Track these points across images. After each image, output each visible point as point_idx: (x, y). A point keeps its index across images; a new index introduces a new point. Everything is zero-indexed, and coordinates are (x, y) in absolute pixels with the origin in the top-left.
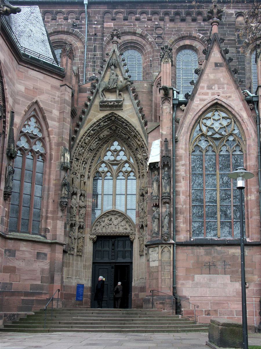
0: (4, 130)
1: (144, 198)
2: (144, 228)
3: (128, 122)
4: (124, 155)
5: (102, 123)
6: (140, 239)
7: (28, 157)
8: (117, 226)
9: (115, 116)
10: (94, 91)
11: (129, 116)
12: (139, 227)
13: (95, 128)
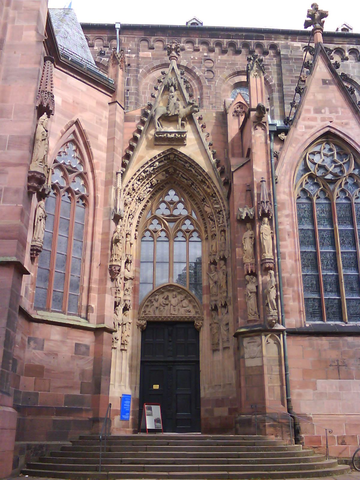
1: (218, 266)
2: (219, 310)
3: (194, 162)
4: (184, 209)
6: (212, 325)
8: (177, 307)
9: (175, 154)
10: (146, 119)
12: (210, 308)
13: (148, 169)
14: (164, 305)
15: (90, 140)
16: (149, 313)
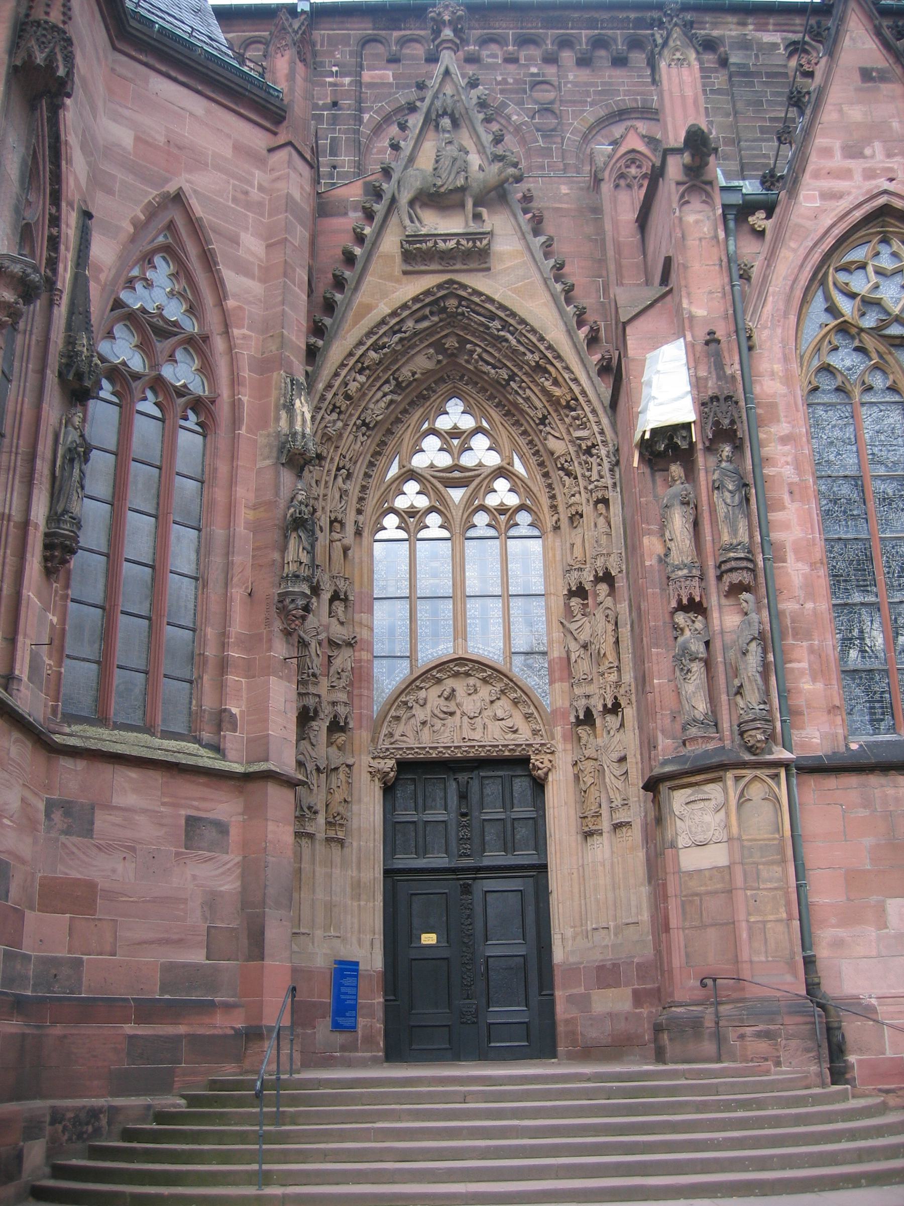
0: (49, 274)
1: (590, 601)
2: (598, 722)
3: (513, 314)
4: (489, 449)
5: (410, 324)
7: (142, 406)
8: (479, 720)
10: (376, 207)
11: (515, 291)
13: (385, 340)
14: (442, 716)
16: (404, 738)
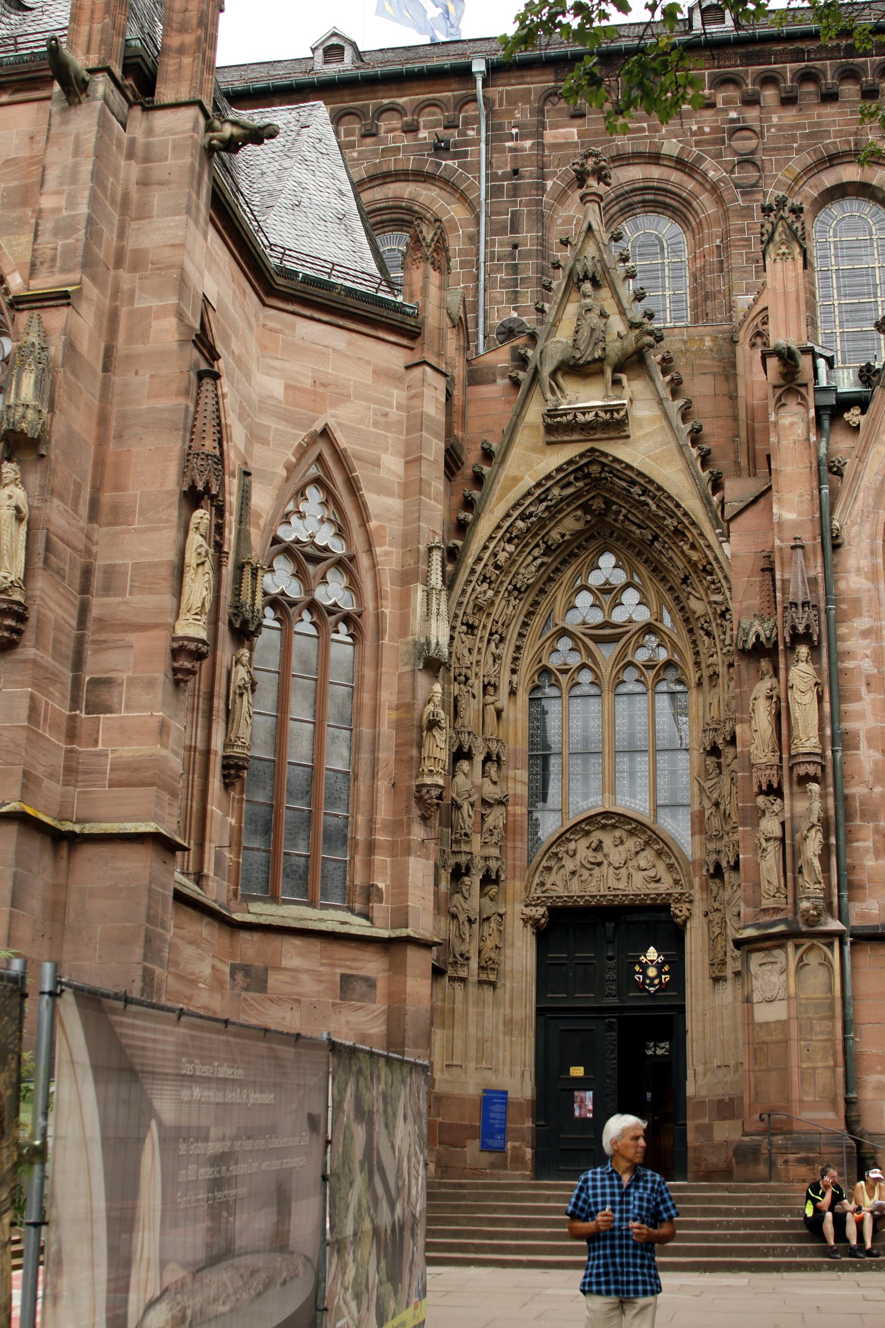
0: (218, 538)
1: (722, 760)
2: (726, 876)
3: (651, 481)
4: (639, 603)
5: (556, 491)
6: (710, 917)
7: (299, 627)
8: (623, 871)
10: (522, 375)
12: (704, 872)
13: (532, 509)
14: (589, 866)
15: (360, 472)
16: (555, 887)
